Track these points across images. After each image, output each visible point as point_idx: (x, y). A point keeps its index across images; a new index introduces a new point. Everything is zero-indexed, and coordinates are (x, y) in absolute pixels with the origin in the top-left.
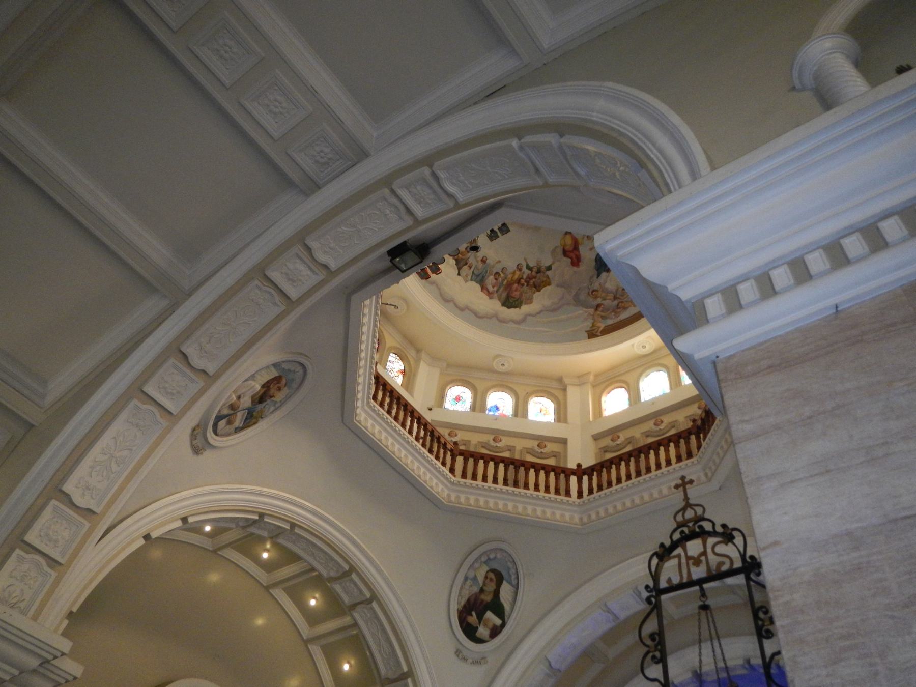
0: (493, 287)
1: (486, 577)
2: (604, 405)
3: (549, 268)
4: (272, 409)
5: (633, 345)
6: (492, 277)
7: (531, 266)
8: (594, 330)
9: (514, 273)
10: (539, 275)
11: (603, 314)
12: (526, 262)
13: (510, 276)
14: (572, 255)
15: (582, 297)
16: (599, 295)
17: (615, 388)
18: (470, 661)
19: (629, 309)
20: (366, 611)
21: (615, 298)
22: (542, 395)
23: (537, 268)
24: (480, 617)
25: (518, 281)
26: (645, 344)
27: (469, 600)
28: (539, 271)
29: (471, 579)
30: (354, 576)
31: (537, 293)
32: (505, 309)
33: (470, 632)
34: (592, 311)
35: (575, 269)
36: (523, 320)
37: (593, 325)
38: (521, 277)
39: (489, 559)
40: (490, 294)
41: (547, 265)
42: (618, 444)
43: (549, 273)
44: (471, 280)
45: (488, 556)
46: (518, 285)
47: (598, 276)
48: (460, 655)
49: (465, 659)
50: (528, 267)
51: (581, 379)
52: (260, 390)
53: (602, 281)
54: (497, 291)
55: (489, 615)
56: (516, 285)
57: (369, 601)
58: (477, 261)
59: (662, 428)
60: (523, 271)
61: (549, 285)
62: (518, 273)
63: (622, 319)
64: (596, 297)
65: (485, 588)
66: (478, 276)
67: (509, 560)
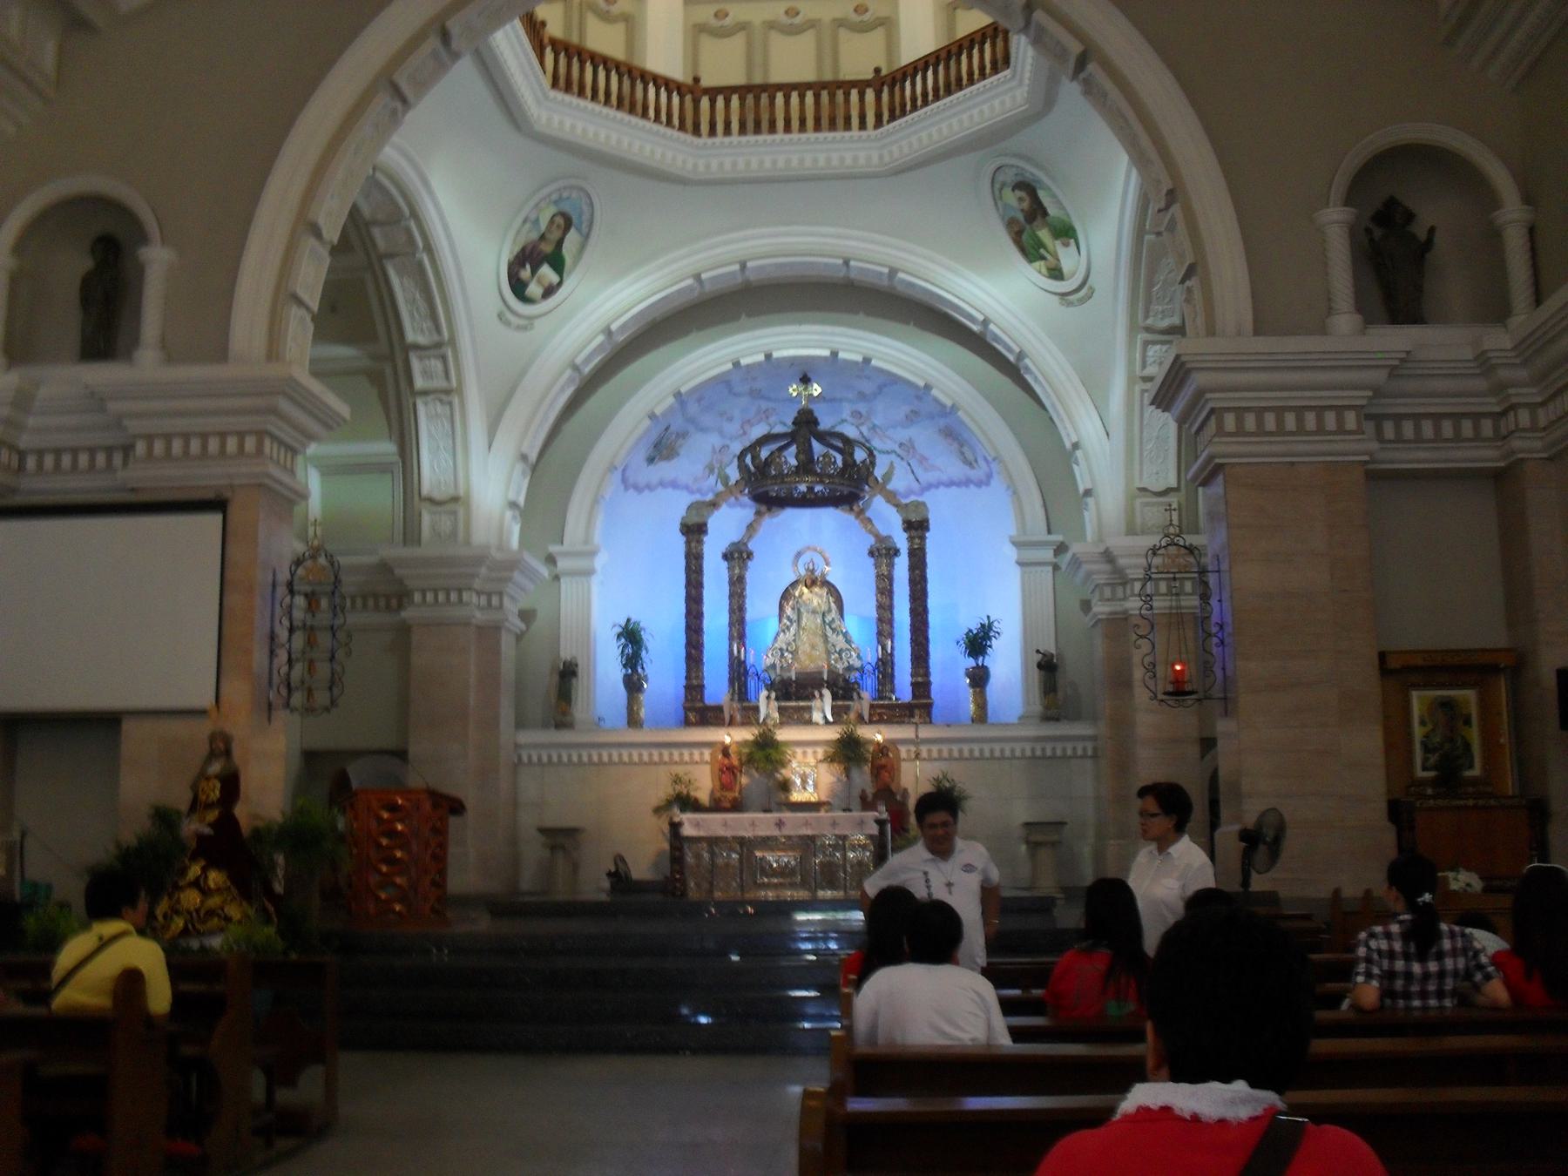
1: (552, 221)
24: (534, 271)
27: (523, 249)
33: (518, 287)
55: (546, 271)
65: (548, 236)
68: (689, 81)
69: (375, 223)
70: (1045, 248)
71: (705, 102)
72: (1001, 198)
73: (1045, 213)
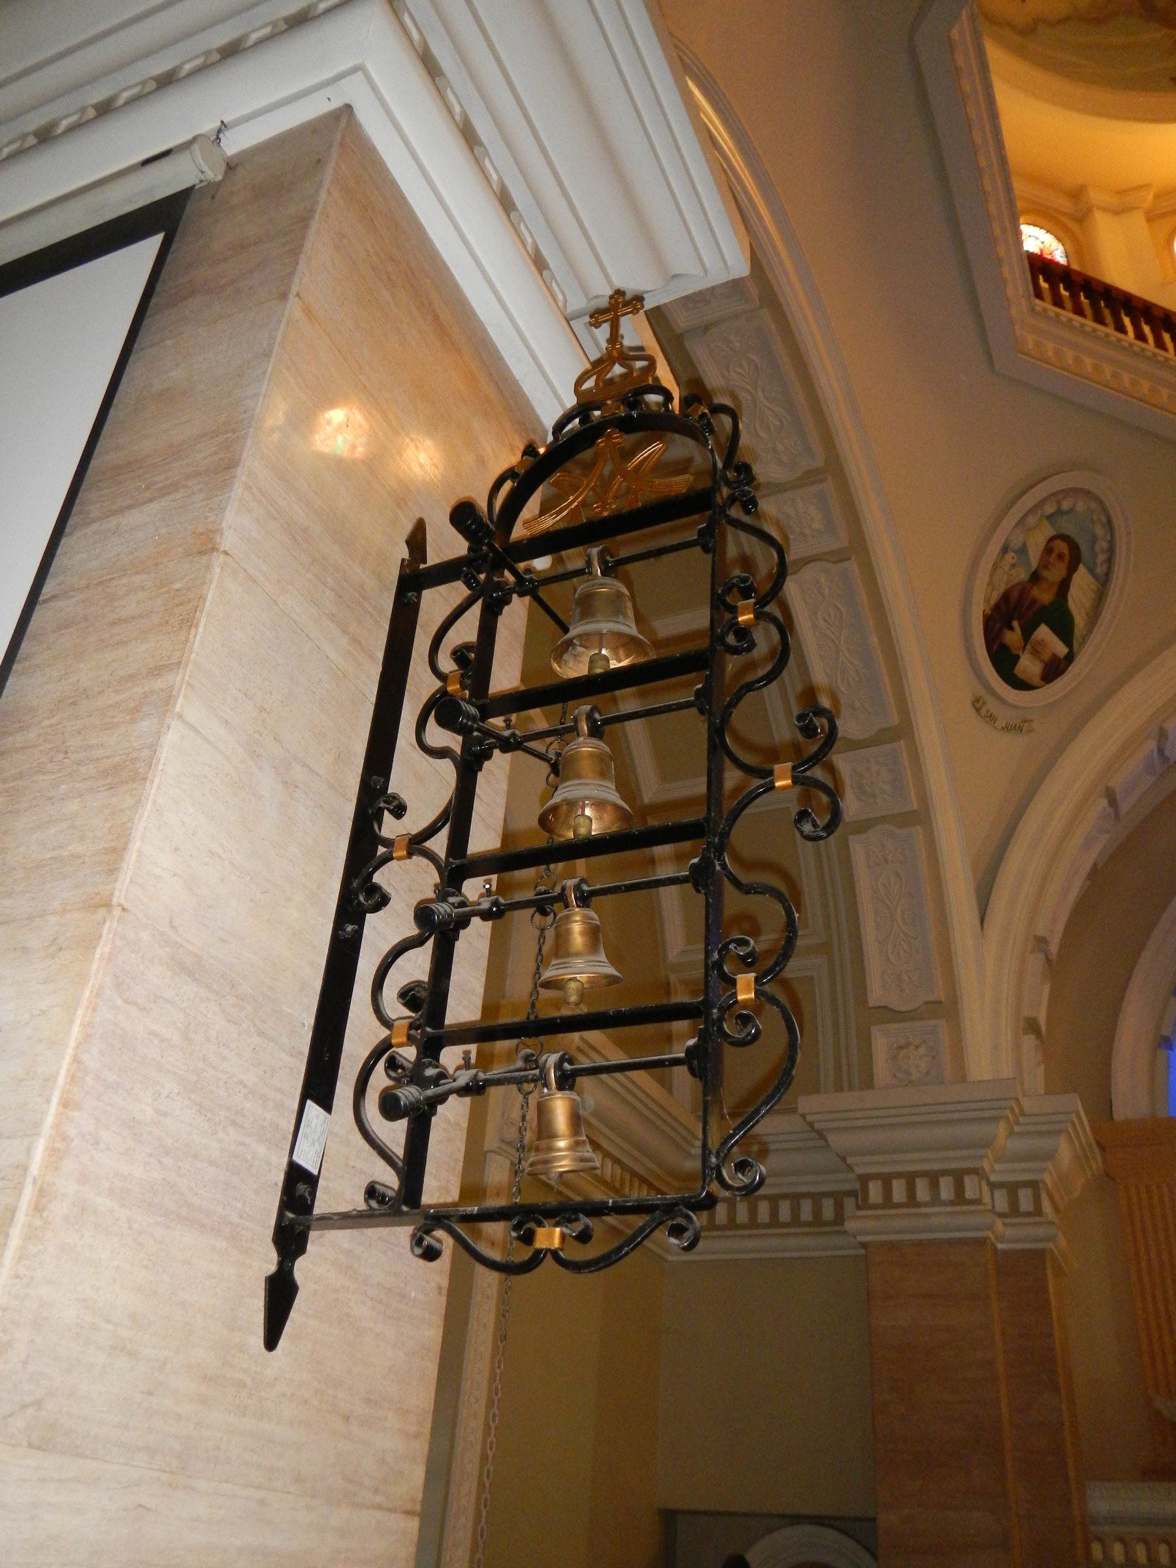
1: (1048, 550)
18: (1001, 723)
24: (1027, 633)
27: (1006, 596)
29: (1014, 552)
45: (1059, 502)
48: (983, 711)
49: (991, 718)
55: (1044, 632)
65: (1046, 574)
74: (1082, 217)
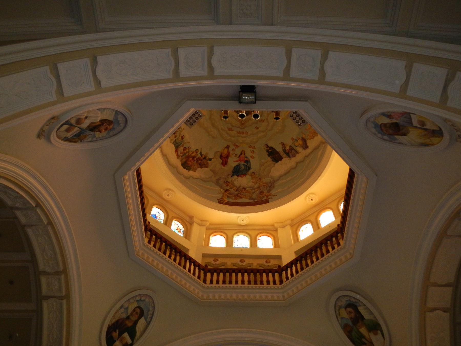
0: (181, 153)
1: (134, 310)
2: (210, 242)
3: (210, 160)
4: (90, 139)
5: (238, 217)
6: (182, 148)
7: (203, 153)
8: (222, 201)
9: (193, 152)
10: (204, 160)
11: (228, 194)
12: (201, 151)
13: (191, 153)
14: (224, 159)
15: (221, 182)
16: (229, 185)
17: (220, 235)
19: (242, 199)
20: (55, 304)
21: (237, 190)
22: (180, 221)
23: (205, 157)
25: (193, 158)
26: (244, 219)
27: (117, 322)
28: (205, 158)
29: (124, 309)
30: (63, 277)
31: (200, 168)
32: (181, 167)
34: (223, 191)
35: (223, 167)
36: (188, 178)
37: (222, 198)
38: (195, 156)
39: (141, 300)
40: (178, 156)
41: (210, 157)
42: (216, 264)
43: (209, 161)
44: (173, 143)
45: (141, 297)
46: (192, 159)
47: (232, 176)
50: (201, 153)
51: (202, 223)
52: (98, 122)
53: (233, 179)
54: (182, 156)
55: (126, 335)
56: (191, 159)
57: (61, 298)
58: (180, 136)
59: (243, 264)
60: (197, 154)
61: (207, 167)
62: (195, 153)
63: (238, 202)
64: (227, 185)
65: (131, 317)
66: (177, 143)
67: (151, 305)
68: (204, 265)
69: (45, 273)
70: (364, 337)
71: (209, 275)
72: (339, 315)
73: (362, 318)
74: (191, 224)
